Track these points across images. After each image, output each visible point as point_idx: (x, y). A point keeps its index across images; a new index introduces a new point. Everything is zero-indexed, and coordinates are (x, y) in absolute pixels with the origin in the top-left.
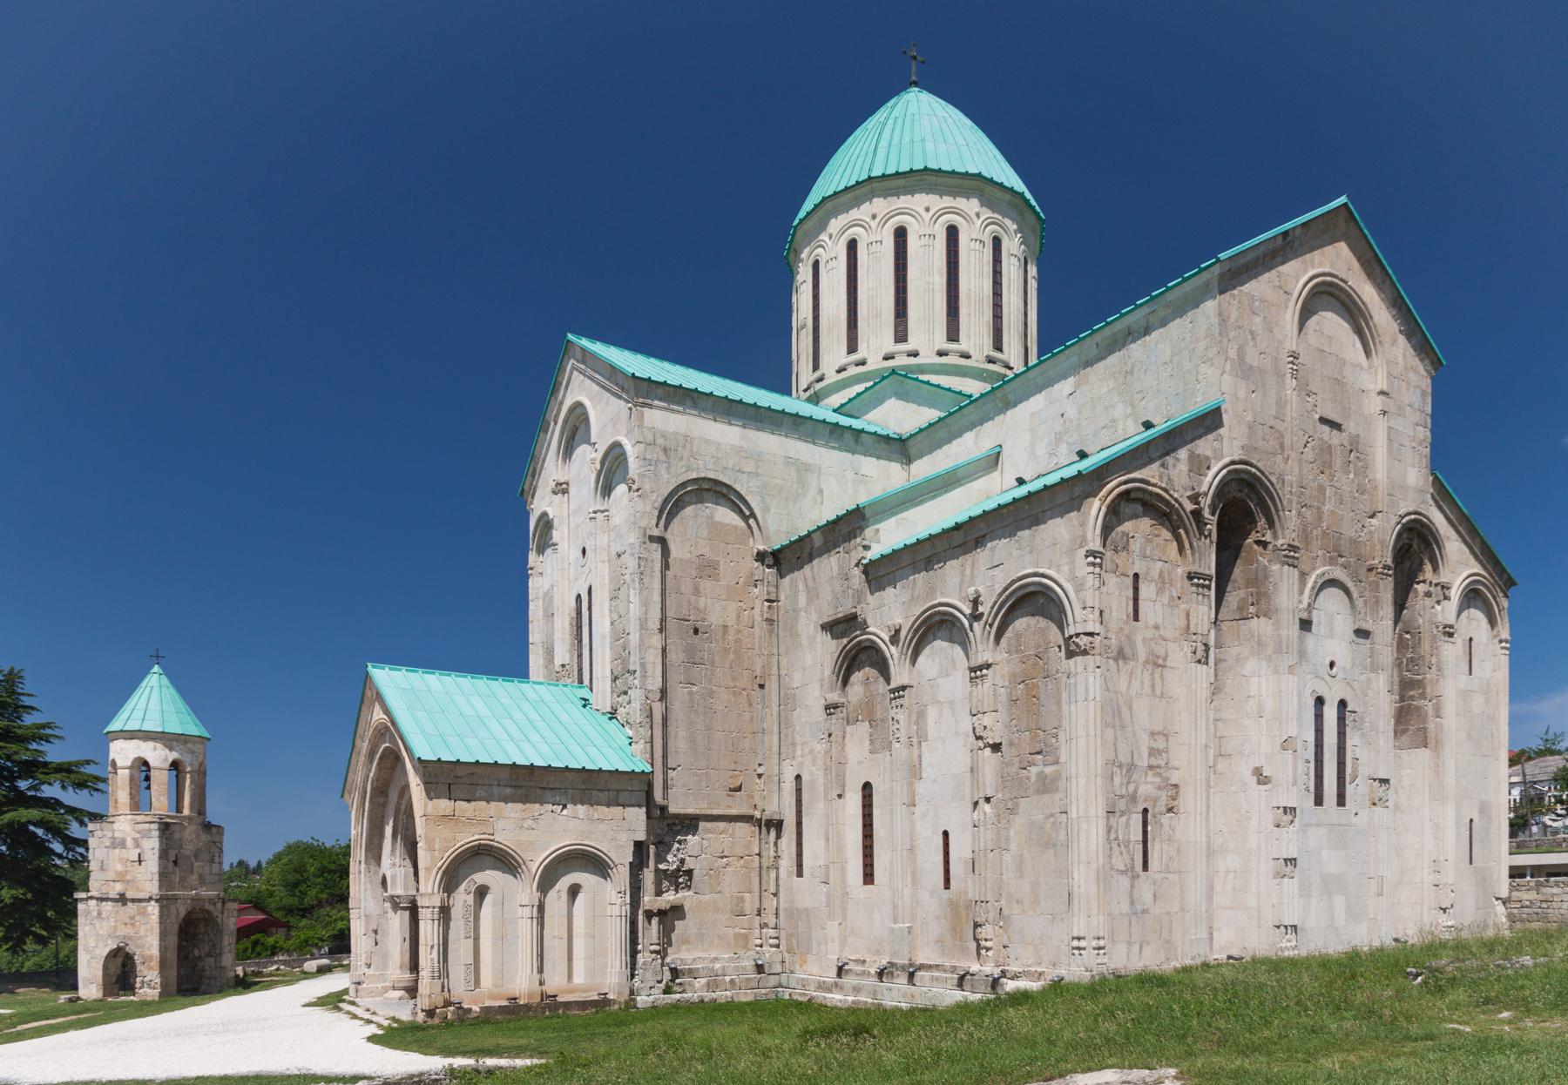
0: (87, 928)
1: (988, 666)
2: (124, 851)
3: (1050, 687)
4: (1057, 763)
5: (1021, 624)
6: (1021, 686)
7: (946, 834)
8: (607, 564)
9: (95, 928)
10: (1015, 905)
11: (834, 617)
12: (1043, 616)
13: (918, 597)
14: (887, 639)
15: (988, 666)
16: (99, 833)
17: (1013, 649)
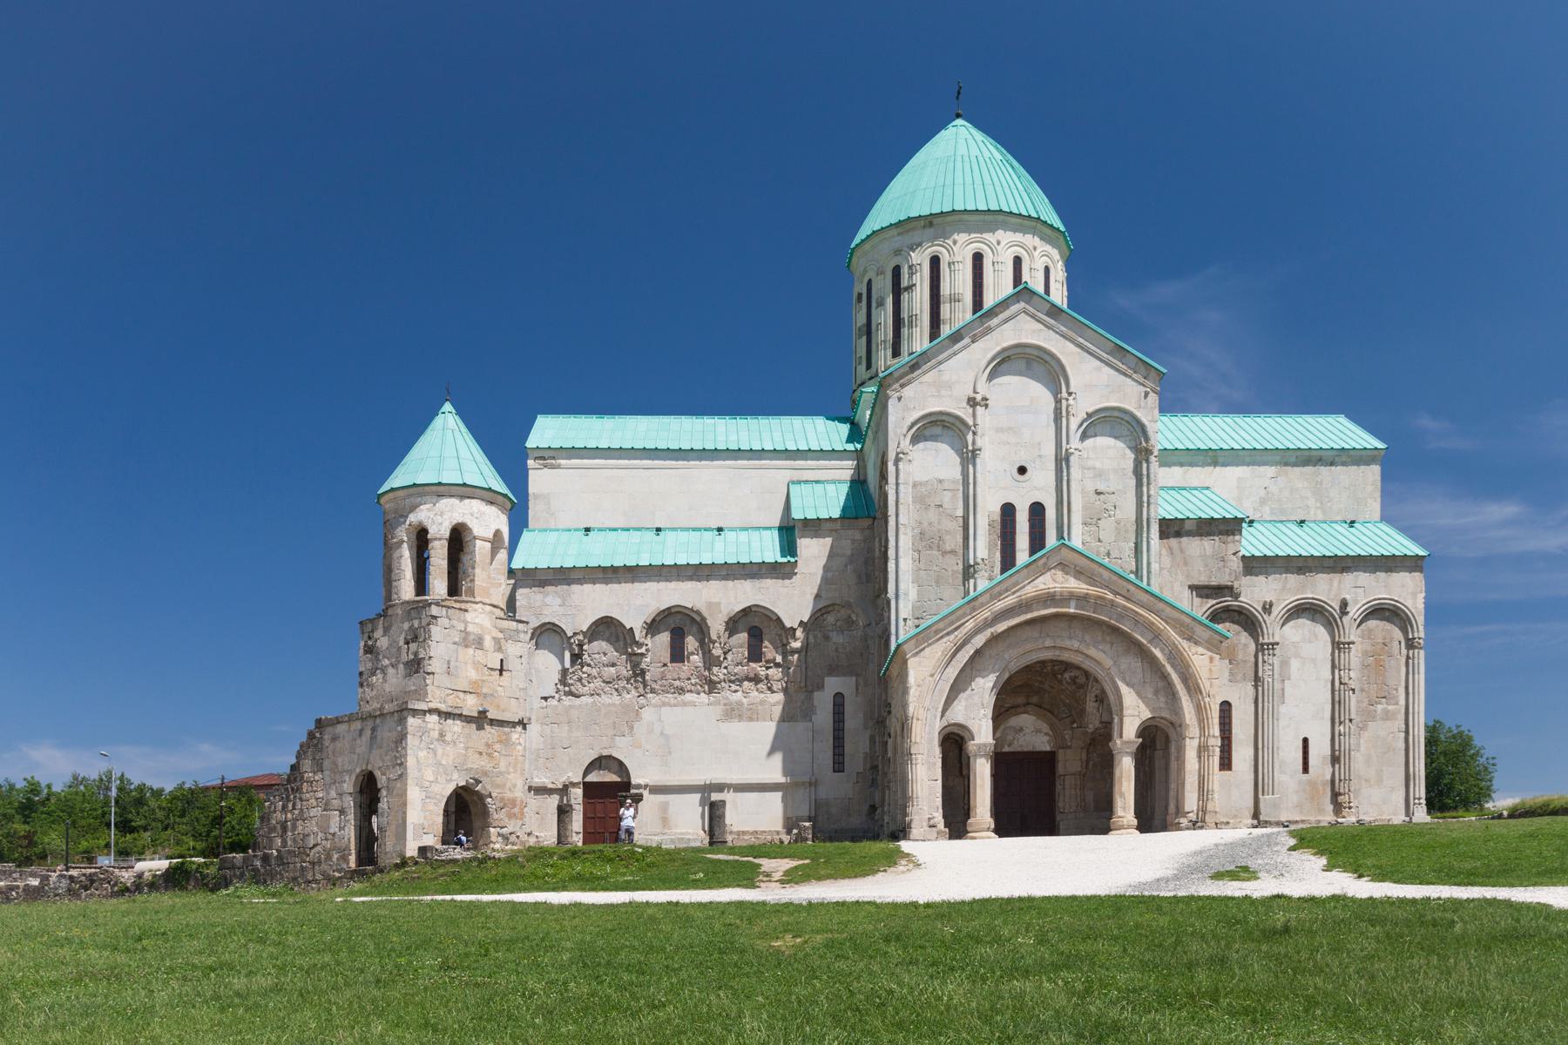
0: (422, 754)
1: (1353, 643)
2: (480, 652)
3: (1392, 662)
4: (1397, 704)
5: (1372, 623)
6: (1371, 658)
7: (1305, 741)
8: (1080, 495)
9: (435, 755)
10: (1363, 783)
11: (1206, 583)
12: (1388, 621)
14: (1260, 609)
15: (1353, 643)
16: (443, 621)
17: (1366, 637)
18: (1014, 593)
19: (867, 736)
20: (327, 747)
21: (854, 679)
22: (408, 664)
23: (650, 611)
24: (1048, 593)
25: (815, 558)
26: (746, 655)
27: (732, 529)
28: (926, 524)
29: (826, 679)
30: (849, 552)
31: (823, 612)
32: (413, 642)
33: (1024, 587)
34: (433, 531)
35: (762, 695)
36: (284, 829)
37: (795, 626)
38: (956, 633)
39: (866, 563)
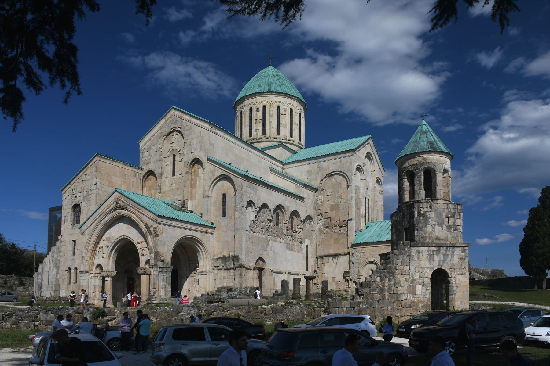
20: (414, 255)
36: (382, 290)
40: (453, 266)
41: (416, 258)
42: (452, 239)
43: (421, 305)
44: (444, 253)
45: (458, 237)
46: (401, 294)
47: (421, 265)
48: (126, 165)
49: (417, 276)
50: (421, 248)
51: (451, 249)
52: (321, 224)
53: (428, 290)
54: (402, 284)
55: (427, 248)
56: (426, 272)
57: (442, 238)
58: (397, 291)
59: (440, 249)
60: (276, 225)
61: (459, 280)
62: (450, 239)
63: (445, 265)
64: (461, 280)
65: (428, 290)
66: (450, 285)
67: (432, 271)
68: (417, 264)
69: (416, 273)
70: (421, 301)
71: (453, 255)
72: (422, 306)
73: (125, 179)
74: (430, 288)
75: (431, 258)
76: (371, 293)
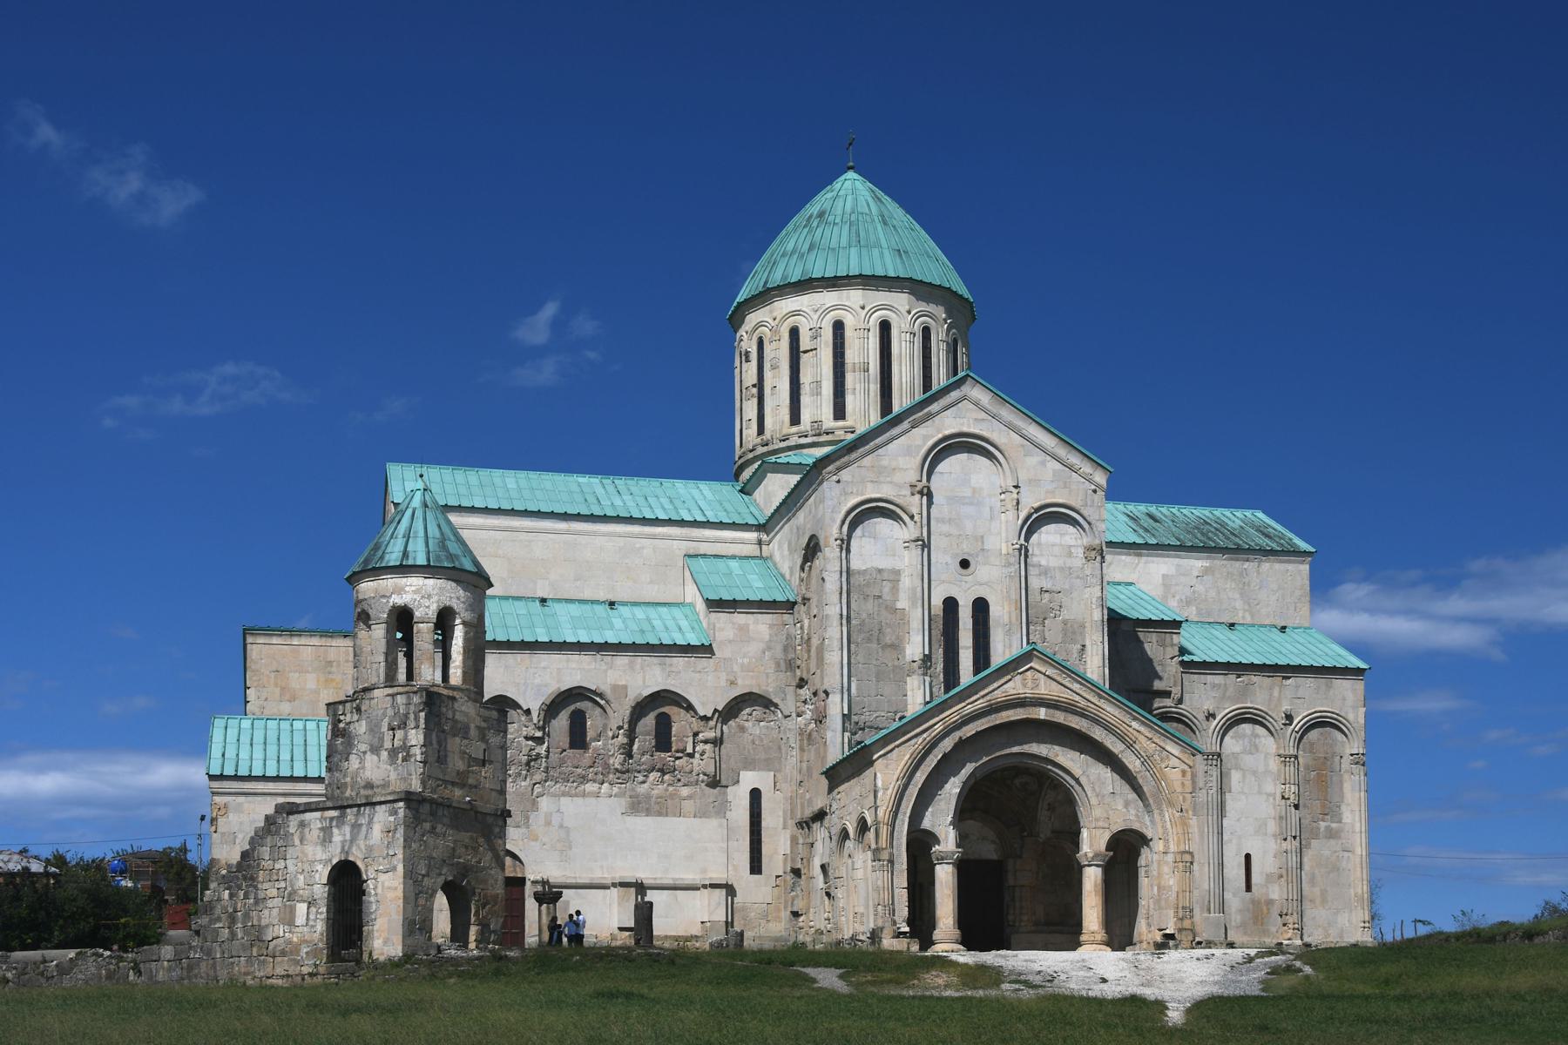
13: (1229, 697)
18: (983, 697)
19: (788, 836)
20: (292, 834)
21: (772, 773)
22: (393, 753)
23: (550, 692)
24: (1019, 698)
25: (730, 642)
26: (653, 744)
27: (624, 604)
28: (864, 616)
29: (741, 772)
30: (767, 637)
31: (739, 700)
32: (399, 728)
33: (993, 691)
34: (417, 614)
35: (671, 789)
36: (232, 919)
37: (709, 715)
38: (925, 735)
39: (785, 649)
40: (371, 851)
41: (297, 842)
42: (398, 781)
43: (305, 950)
44: (353, 821)
45: (411, 775)
46: (267, 926)
47: (306, 855)
48: (331, 637)
49: (301, 881)
50: (308, 816)
51: (368, 808)
52: (809, 715)
53: (321, 913)
54: (270, 903)
55: (317, 814)
56: (317, 871)
57: (378, 783)
58: (260, 919)
59: (345, 813)
60: (573, 745)
61: (383, 886)
62: (393, 782)
63: (354, 849)
64: (386, 884)
65: (321, 913)
66: (364, 897)
67: (330, 868)
68: (300, 855)
69: (299, 876)
70: (306, 941)
71: (370, 822)
72: (307, 953)
73: (330, 673)
74: (324, 909)
75: (327, 832)
76: (212, 926)
